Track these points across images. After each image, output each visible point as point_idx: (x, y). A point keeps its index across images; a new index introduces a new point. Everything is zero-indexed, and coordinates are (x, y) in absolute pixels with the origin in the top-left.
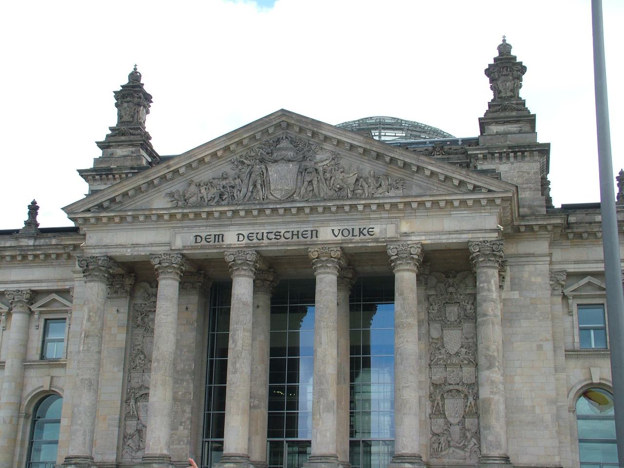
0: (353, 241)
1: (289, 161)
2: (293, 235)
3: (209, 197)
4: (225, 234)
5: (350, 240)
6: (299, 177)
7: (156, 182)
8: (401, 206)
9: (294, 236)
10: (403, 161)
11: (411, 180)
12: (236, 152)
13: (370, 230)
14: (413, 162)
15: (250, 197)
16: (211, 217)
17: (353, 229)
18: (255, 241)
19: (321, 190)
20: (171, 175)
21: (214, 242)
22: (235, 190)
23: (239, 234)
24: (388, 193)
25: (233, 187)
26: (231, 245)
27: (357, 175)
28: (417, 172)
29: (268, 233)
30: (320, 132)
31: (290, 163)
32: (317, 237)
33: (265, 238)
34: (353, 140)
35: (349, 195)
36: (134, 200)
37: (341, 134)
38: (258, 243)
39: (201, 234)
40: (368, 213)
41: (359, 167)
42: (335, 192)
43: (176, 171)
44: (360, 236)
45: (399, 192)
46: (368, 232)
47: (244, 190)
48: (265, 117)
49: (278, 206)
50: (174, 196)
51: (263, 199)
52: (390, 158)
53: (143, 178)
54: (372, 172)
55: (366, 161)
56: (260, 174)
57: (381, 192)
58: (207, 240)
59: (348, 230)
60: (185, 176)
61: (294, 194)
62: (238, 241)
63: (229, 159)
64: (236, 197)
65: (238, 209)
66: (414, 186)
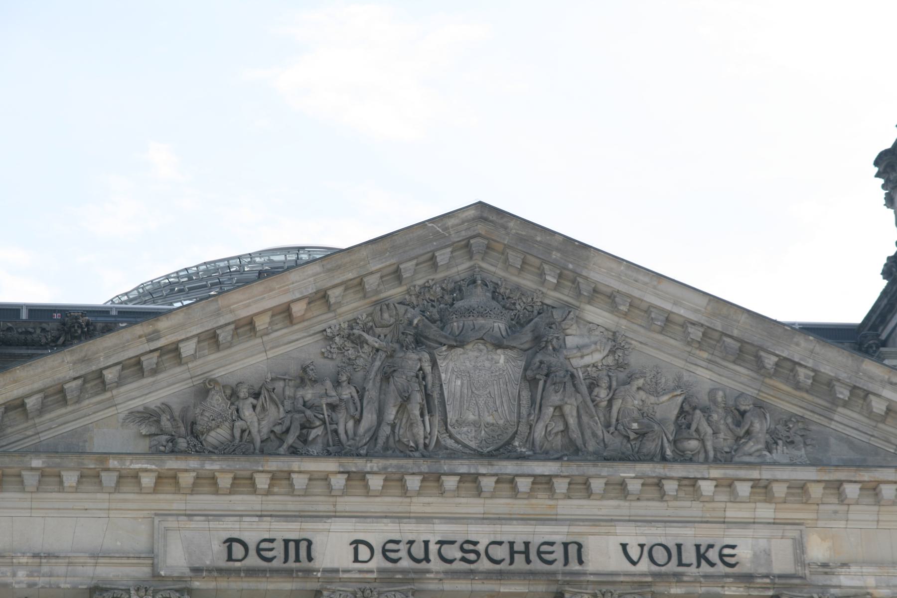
0: (685, 579)
1: (498, 345)
2: (512, 553)
3: (265, 430)
4: (317, 540)
5: (675, 575)
6: (525, 394)
7: (109, 375)
8: (816, 491)
9: (516, 556)
10: (814, 370)
11: (825, 422)
12: (339, 311)
13: (727, 551)
14: (843, 376)
15: (388, 438)
16: (276, 489)
17: (679, 546)
18: (406, 563)
19: (588, 433)
20: (155, 360)
21: (286, 560)
22: (340, 415)
23: (356, 543)
24: (770, 452)
25: (333, 407)
26: (336, 571)
27: (680, 399)
28: (846, 404)
29: (441, 543)
30: (584, 273)
31: (499, 351)
32: (581, 562)
33: (433, 555)
34: (675, 303)
35: (668, 452)
36: (35, 426)
37: (646, 284)
38: (416, 572)
39: (245, 537)
40: (723, 505)
41: (680, 378)
42: (625, 441)
43: (173, 351)
44: (699, 566)
45: (798, 453)
46: (721, 556)
47: (369, 419)
48: (432, 220)
49: (483, 470)
50: (158, 422)
51: (426, 446)
52: (776, 359)
53: (75, 363)
54: (721, 393)
55: (704, 364)
56: (417, 377)
57: (753, 449)
58: (263, 553)
59: (666, 548)
60: (190, 365)
61: (513, 438)
62: (356, 560)
63: (319, 328)
64: (343, 436)
65: (368, 469)
66: (832, 441)
